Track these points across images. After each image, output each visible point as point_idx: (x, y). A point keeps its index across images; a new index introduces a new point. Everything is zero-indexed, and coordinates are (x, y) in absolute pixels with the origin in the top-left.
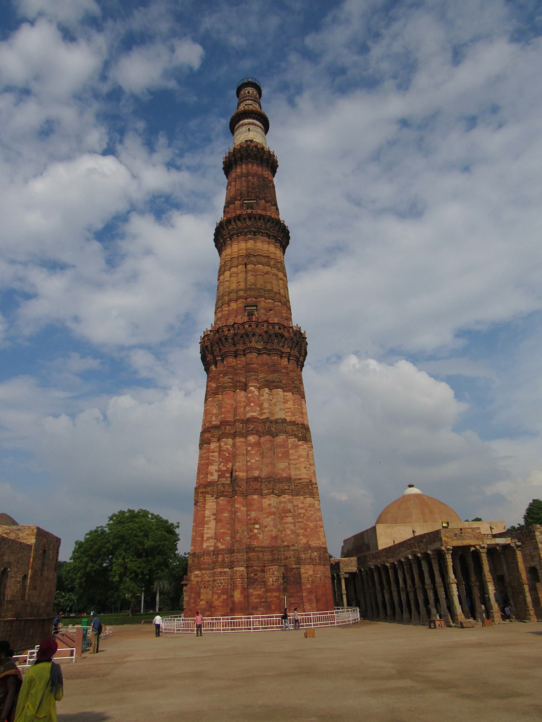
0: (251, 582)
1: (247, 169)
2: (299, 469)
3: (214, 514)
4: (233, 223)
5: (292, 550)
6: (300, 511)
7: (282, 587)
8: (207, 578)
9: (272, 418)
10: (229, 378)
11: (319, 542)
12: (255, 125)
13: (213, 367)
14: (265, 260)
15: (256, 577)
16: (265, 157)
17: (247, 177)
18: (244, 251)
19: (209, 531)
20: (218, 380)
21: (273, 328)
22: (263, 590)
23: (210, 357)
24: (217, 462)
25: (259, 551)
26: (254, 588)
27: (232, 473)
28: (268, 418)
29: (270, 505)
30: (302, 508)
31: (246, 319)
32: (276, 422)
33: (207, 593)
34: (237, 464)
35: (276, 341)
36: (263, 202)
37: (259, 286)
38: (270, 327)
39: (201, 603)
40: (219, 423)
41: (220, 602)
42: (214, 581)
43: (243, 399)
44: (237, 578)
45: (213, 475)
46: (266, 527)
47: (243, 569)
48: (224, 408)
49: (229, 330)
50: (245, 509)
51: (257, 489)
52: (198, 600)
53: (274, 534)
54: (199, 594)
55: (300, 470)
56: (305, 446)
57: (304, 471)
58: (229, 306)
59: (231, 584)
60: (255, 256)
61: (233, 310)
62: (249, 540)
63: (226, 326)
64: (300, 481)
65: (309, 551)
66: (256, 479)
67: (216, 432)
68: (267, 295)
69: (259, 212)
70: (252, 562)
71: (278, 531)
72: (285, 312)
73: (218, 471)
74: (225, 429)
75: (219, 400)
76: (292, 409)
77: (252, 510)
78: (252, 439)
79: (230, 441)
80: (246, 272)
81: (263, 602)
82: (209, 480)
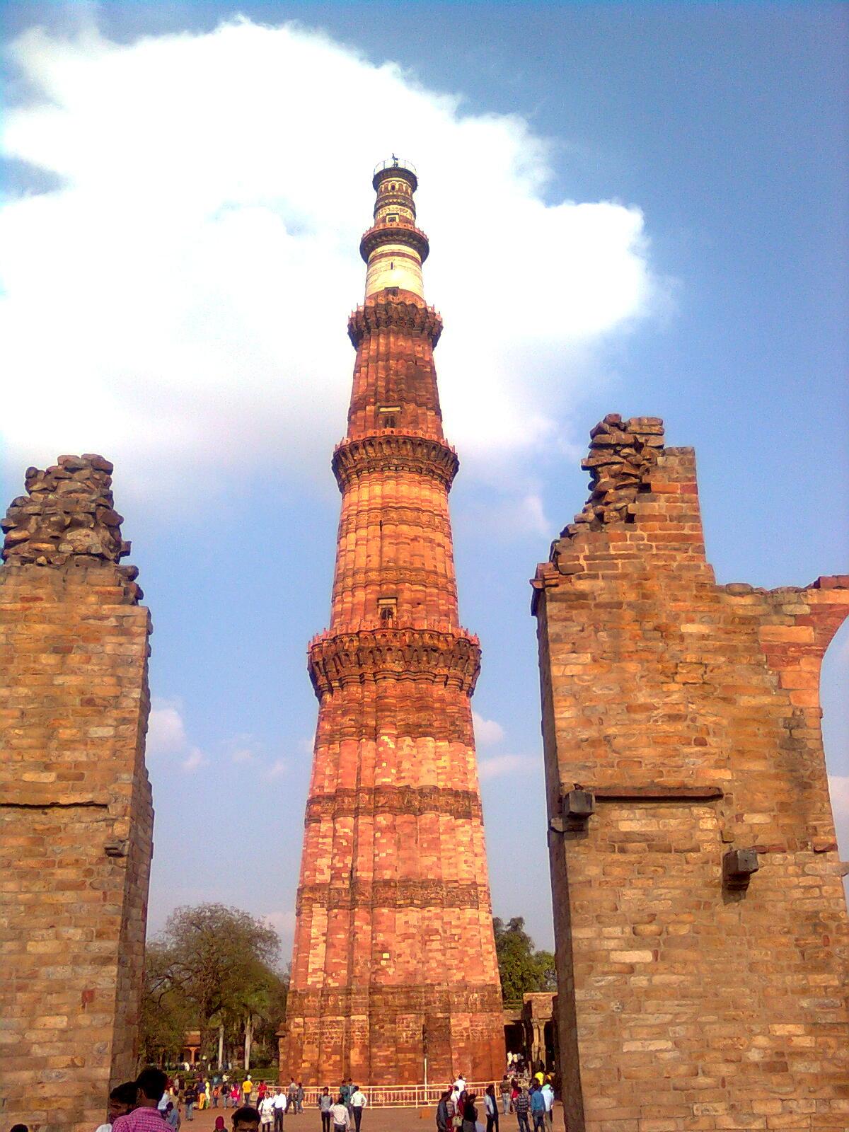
0: (374, 1039)
1: (387, 345)
2: (456, 866)
3: (324, 934)
4: (361, 450)
5: (437, 992)
6: (454, 931)
7: (421, 1046)
8: (312, 1030)
9: (414, 786)
10: (350, 720)
11: (482, 978)
12: (403, 255)
13: (327, 697)
14: (410, 515)
15: (382, 1030)
16: (418, 321)
17: (387, 360)
18: (379, 501)
19: (316, 959)
20: (334, 719)
21: (421, 637)
22: (392, 1049)
23: (322, 681)
24: (330, 853)
25: (387, 993)
26: (378, 1047)
27: (351, 872)
28: (408, 787)
29: (406, 922)
30: (457, 927)
31: (378, 624)
32: (421, 792)
33: (312, 1052)
34: (359, 859)
35: (424, 659)
36: (412, 406)
37: (401, 563)
38: (416, 636)
39: (303, 1065)
40: (334, 791)
41: (330, 1065)
42: (322, 1034)
43: (372, 755)
44: (354, 1032)
45: (323, 874)
46: (400, 955)
47: (364, 1017)
48: (343, 768)
49: (352, 640)
50: (370, 928)
51: (387, 899)
52: (300, 1061)
53: (411, 968)
54: (301, 1052)
55: (456, 867)
56: (467, 827)
57: (464, 866)
58: (353, 596)
59: (346, 1040)
60: (396, 508)
61: (358, 604)
62: (374, 976)
63: (347, 634)
64: (456, 885)
65: (465, 993)
66: (387, 883)
67: (330, 806)
68: (413, 578)
69: (404, 431)
70: (376, 1008)
71: (418, 962)
72: (444, 602)
73: (332, 867)
74: (344, 802)
75: (335, 754)
76: (448, 768)
77: (380, 931)
78: (383, 820)
79: (350, 820)
80: (382, 538)
81: (391, 1067)
82: (317, 882)
